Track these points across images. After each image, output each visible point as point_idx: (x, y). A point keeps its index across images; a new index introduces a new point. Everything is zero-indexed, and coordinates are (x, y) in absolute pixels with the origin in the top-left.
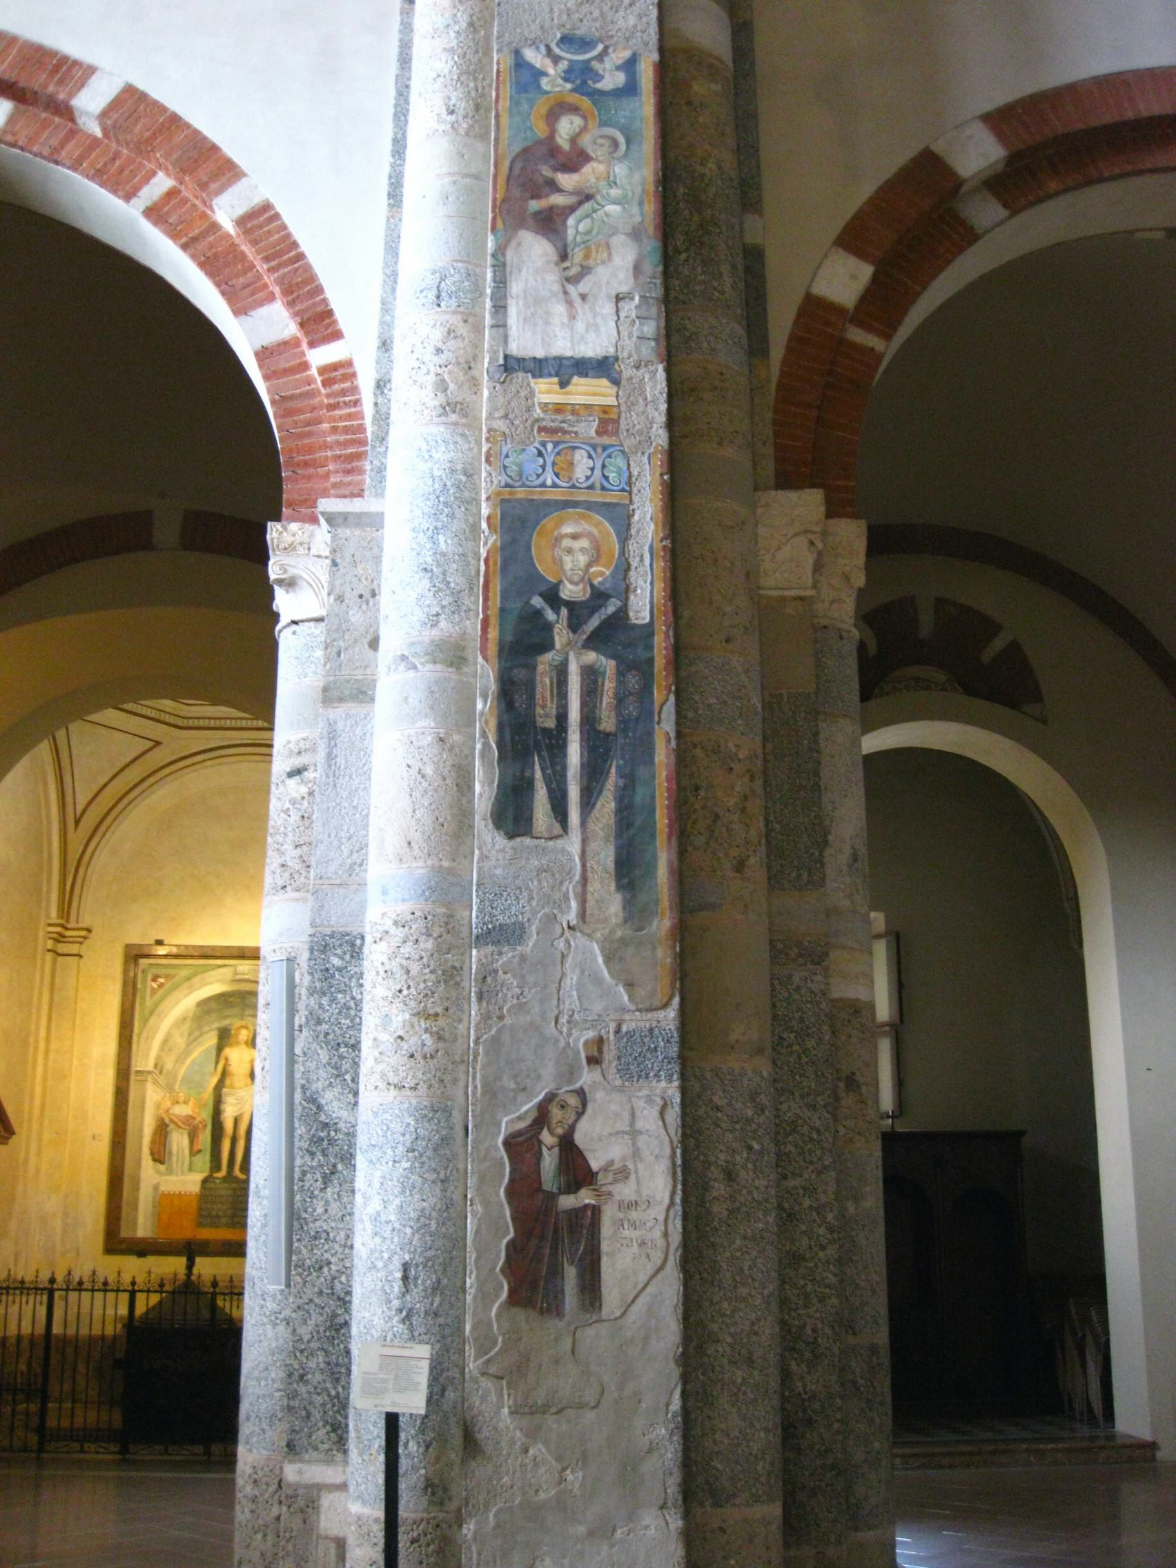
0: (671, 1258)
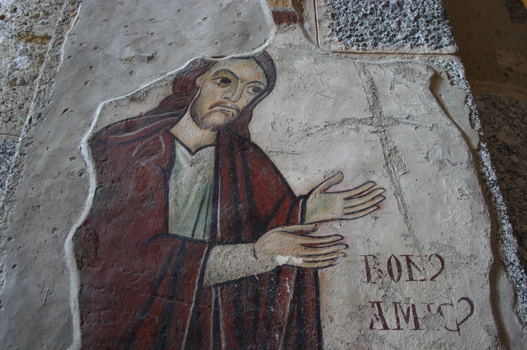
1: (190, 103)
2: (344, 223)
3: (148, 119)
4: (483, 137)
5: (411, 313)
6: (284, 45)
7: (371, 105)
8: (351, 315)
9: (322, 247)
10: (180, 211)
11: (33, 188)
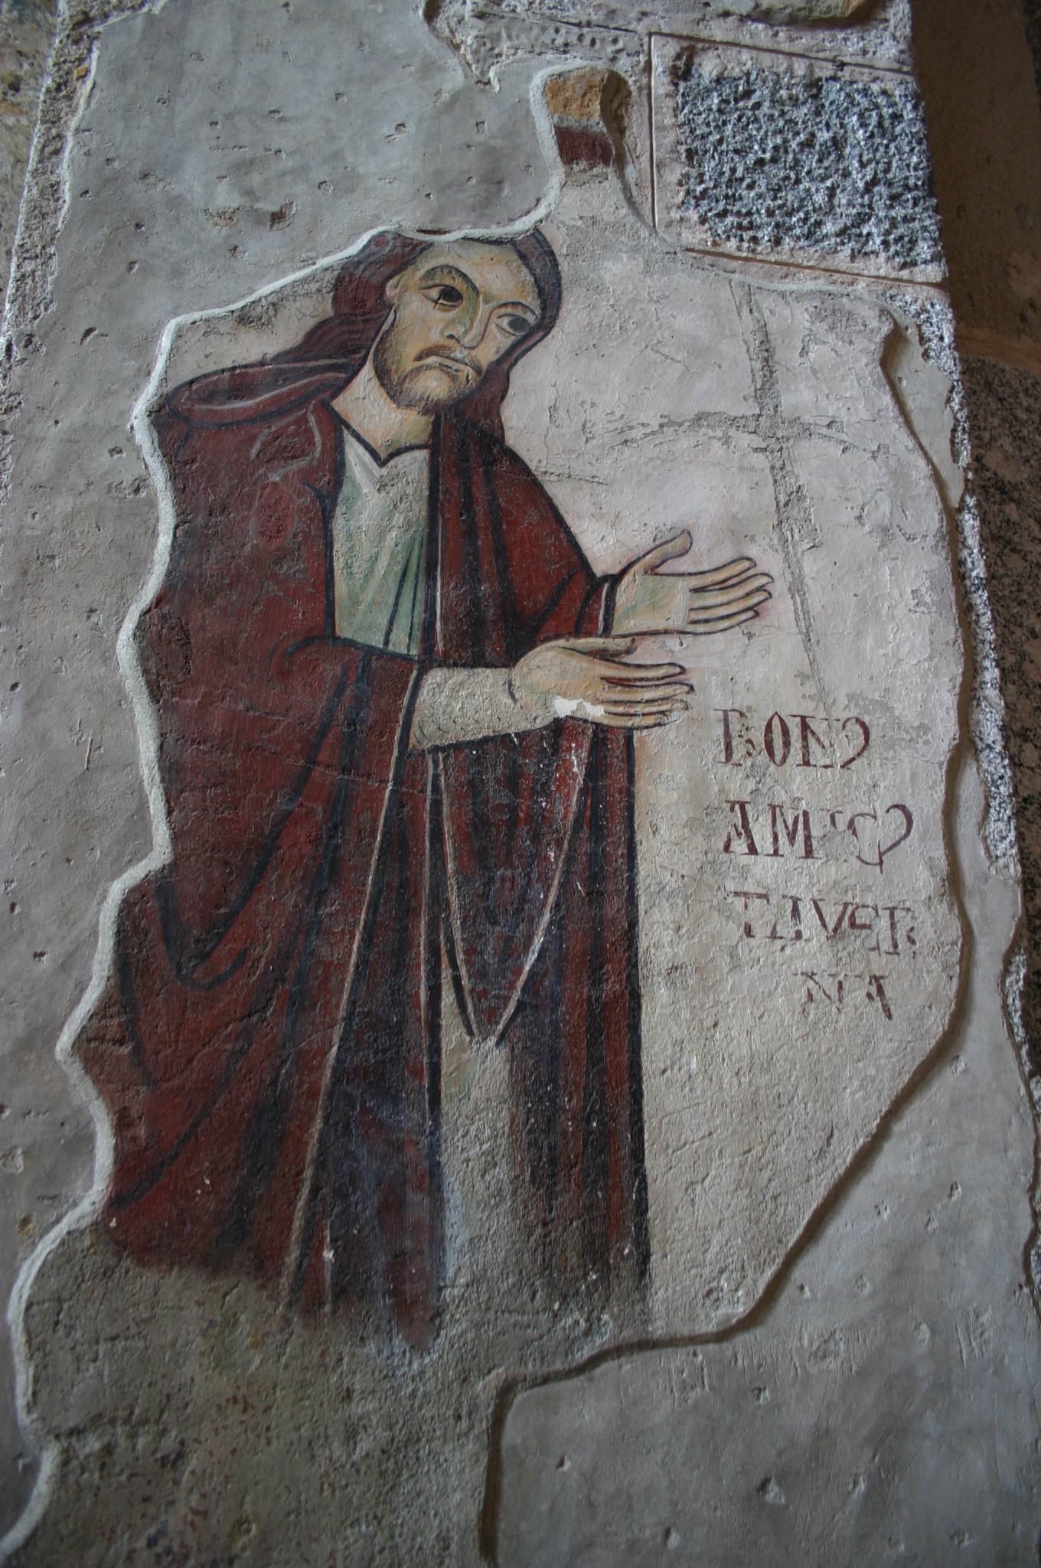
0: (986, 1001)
1: (373, 340)
2: (688, 640)
3: (280, 372)
4: (973, 482)
5: (800, 826)
6: (581, 218)
7: (758, 387)
8: (692, 824)
9: (642, 687)
10: (357, 589)
11: (34, 515)
